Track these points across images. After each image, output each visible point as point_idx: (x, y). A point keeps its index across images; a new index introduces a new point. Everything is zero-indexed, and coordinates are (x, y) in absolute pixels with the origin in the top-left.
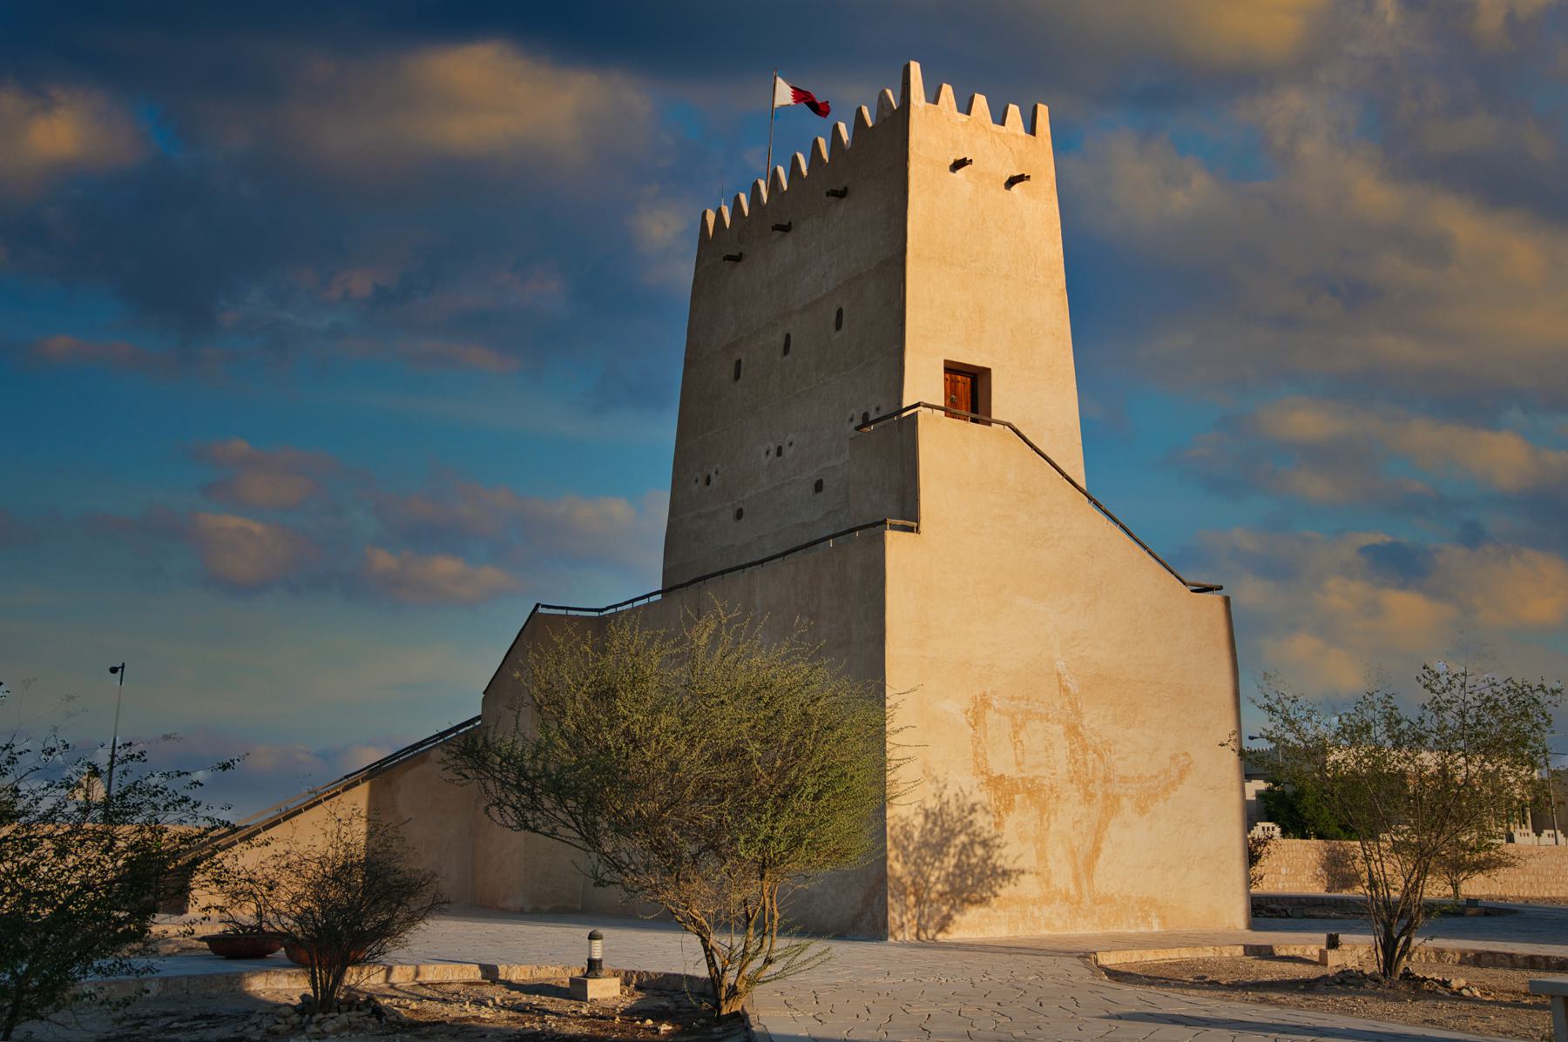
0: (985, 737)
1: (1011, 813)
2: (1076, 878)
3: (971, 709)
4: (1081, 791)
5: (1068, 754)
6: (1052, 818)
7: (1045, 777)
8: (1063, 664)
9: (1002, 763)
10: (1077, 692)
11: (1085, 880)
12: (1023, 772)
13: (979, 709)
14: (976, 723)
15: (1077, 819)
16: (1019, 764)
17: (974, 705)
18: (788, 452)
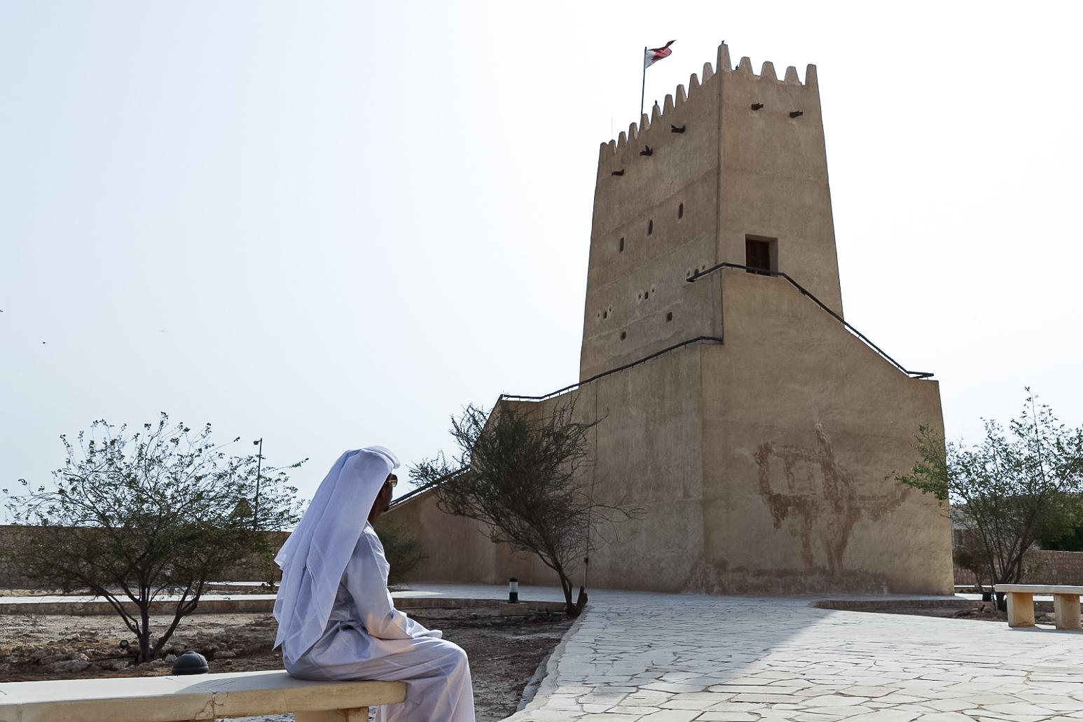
0: (768, 470)
1: (785, 518)
2: (830, 559)
3: (758, 452)
6: (813, 522)
7: (808, 496)
9: (779, 487)
10: (830, 442)
13: (763, 454)
14: (761, 461)
15: (830, 522)
16: (790, 487)
18: (652, 296)
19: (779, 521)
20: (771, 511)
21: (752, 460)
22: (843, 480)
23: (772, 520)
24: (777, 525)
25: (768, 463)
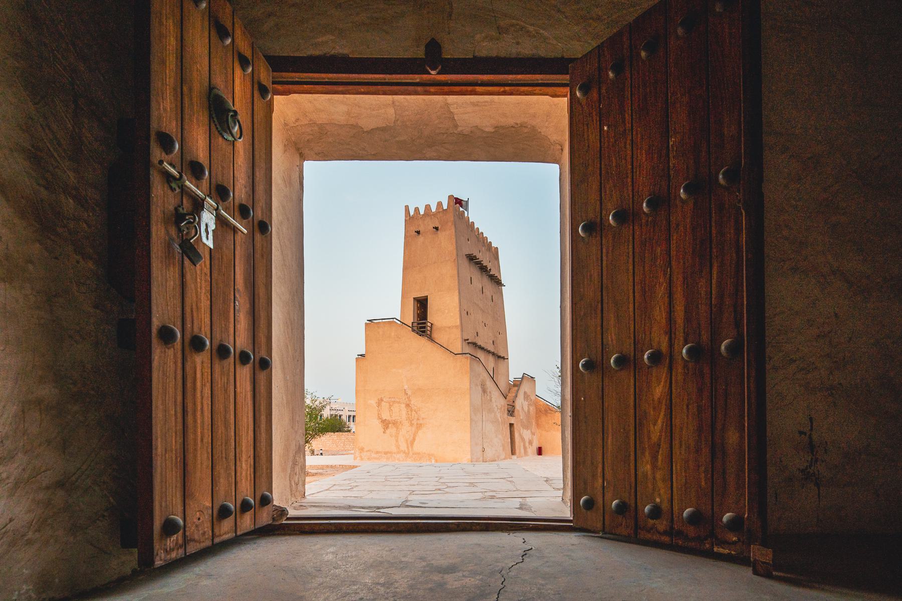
2: (408, 447)
9: (386, 416)
21: (375, 405)
22: (415, 411)
23: (383, 430)
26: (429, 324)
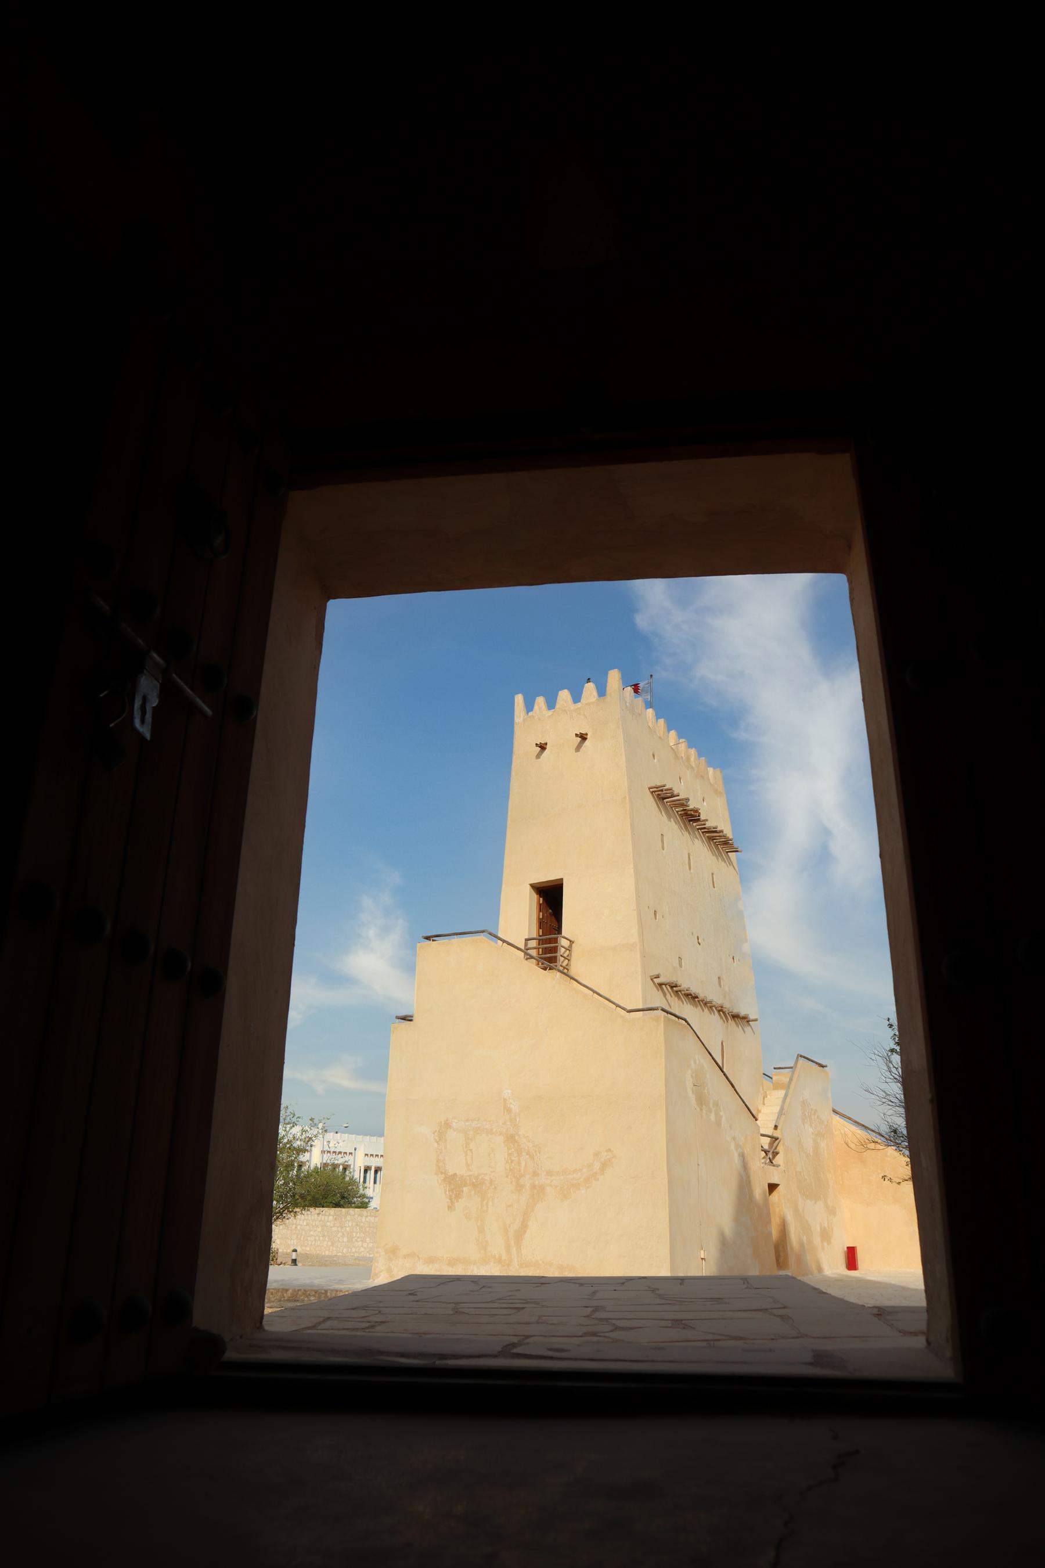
0: (445, 1148)
1: (460, 1200)
2: (508, 1248)
3: (437, 1130)
4: (514, 1183)
5: (506, 1157)
6: (490, 1204)
7: (486, 1174)
8: (509, 1091)
9: (456, 1166)
11: (514, 1249)
12: (471, 1171)
14: (440, 1139)
16: (468, 1165)
17: (439, 1128)
19: (452, 1203)
20: (445, 1192)
24: (451, 1208)
25: (446, 1140)
26: (564, 942)
